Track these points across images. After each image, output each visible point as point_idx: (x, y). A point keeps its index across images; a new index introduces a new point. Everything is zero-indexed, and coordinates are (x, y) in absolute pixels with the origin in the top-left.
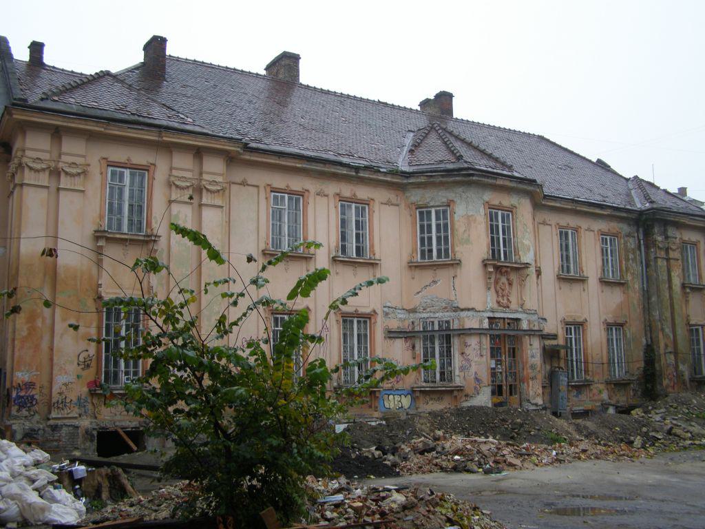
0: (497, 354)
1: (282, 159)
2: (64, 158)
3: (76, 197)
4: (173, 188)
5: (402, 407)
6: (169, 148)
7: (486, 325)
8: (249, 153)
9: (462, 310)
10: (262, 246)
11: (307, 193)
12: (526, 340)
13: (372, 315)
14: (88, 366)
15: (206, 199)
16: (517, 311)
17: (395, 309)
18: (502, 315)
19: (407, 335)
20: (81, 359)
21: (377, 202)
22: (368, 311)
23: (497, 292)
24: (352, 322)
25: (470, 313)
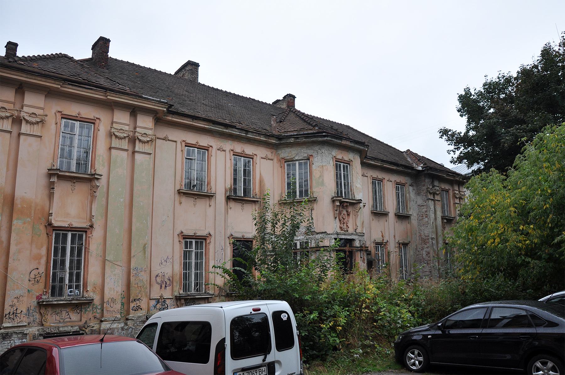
1: (195, 121)
2: (25, 109)
4: (114, 137)
6: (111, 106)
8: (171, 115)
9: (318, 233)
10: (178, 187)
11: (211, 148)
14: (38, 282)
15: (139, 147)
16: (352, 234)
20: (32, 276)
23: (340, 220)
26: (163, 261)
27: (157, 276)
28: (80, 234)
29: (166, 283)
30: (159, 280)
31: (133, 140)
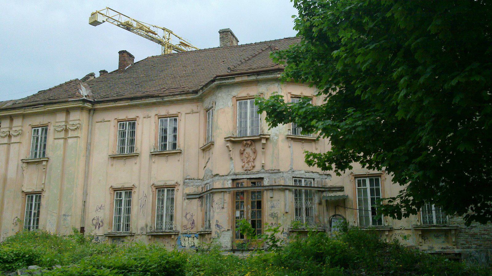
0: (241, 207)
3: (16, 146)
5: (194, 245)
7: (229, 184)
8: (98, 104)
12: (267, 196)
13: (175, 185)
17: (194, 180)
18: (245, 177)
19: (200, 197)
21: (183, 114)
22: (173, 183)
24: (163, 191)
25: (217, 178)
26: (98, 208)
27: (93, 219)
28: (38, 195)
29: (99, 225)
30: (95, 222)
31: (66, 130)
